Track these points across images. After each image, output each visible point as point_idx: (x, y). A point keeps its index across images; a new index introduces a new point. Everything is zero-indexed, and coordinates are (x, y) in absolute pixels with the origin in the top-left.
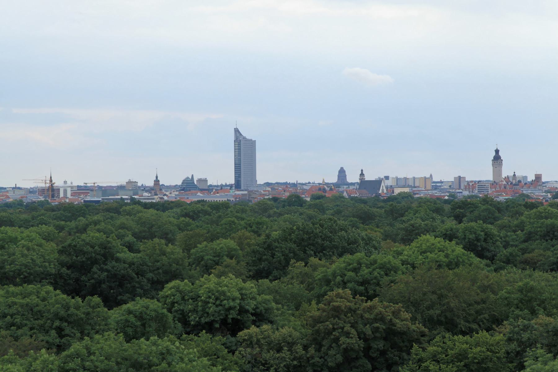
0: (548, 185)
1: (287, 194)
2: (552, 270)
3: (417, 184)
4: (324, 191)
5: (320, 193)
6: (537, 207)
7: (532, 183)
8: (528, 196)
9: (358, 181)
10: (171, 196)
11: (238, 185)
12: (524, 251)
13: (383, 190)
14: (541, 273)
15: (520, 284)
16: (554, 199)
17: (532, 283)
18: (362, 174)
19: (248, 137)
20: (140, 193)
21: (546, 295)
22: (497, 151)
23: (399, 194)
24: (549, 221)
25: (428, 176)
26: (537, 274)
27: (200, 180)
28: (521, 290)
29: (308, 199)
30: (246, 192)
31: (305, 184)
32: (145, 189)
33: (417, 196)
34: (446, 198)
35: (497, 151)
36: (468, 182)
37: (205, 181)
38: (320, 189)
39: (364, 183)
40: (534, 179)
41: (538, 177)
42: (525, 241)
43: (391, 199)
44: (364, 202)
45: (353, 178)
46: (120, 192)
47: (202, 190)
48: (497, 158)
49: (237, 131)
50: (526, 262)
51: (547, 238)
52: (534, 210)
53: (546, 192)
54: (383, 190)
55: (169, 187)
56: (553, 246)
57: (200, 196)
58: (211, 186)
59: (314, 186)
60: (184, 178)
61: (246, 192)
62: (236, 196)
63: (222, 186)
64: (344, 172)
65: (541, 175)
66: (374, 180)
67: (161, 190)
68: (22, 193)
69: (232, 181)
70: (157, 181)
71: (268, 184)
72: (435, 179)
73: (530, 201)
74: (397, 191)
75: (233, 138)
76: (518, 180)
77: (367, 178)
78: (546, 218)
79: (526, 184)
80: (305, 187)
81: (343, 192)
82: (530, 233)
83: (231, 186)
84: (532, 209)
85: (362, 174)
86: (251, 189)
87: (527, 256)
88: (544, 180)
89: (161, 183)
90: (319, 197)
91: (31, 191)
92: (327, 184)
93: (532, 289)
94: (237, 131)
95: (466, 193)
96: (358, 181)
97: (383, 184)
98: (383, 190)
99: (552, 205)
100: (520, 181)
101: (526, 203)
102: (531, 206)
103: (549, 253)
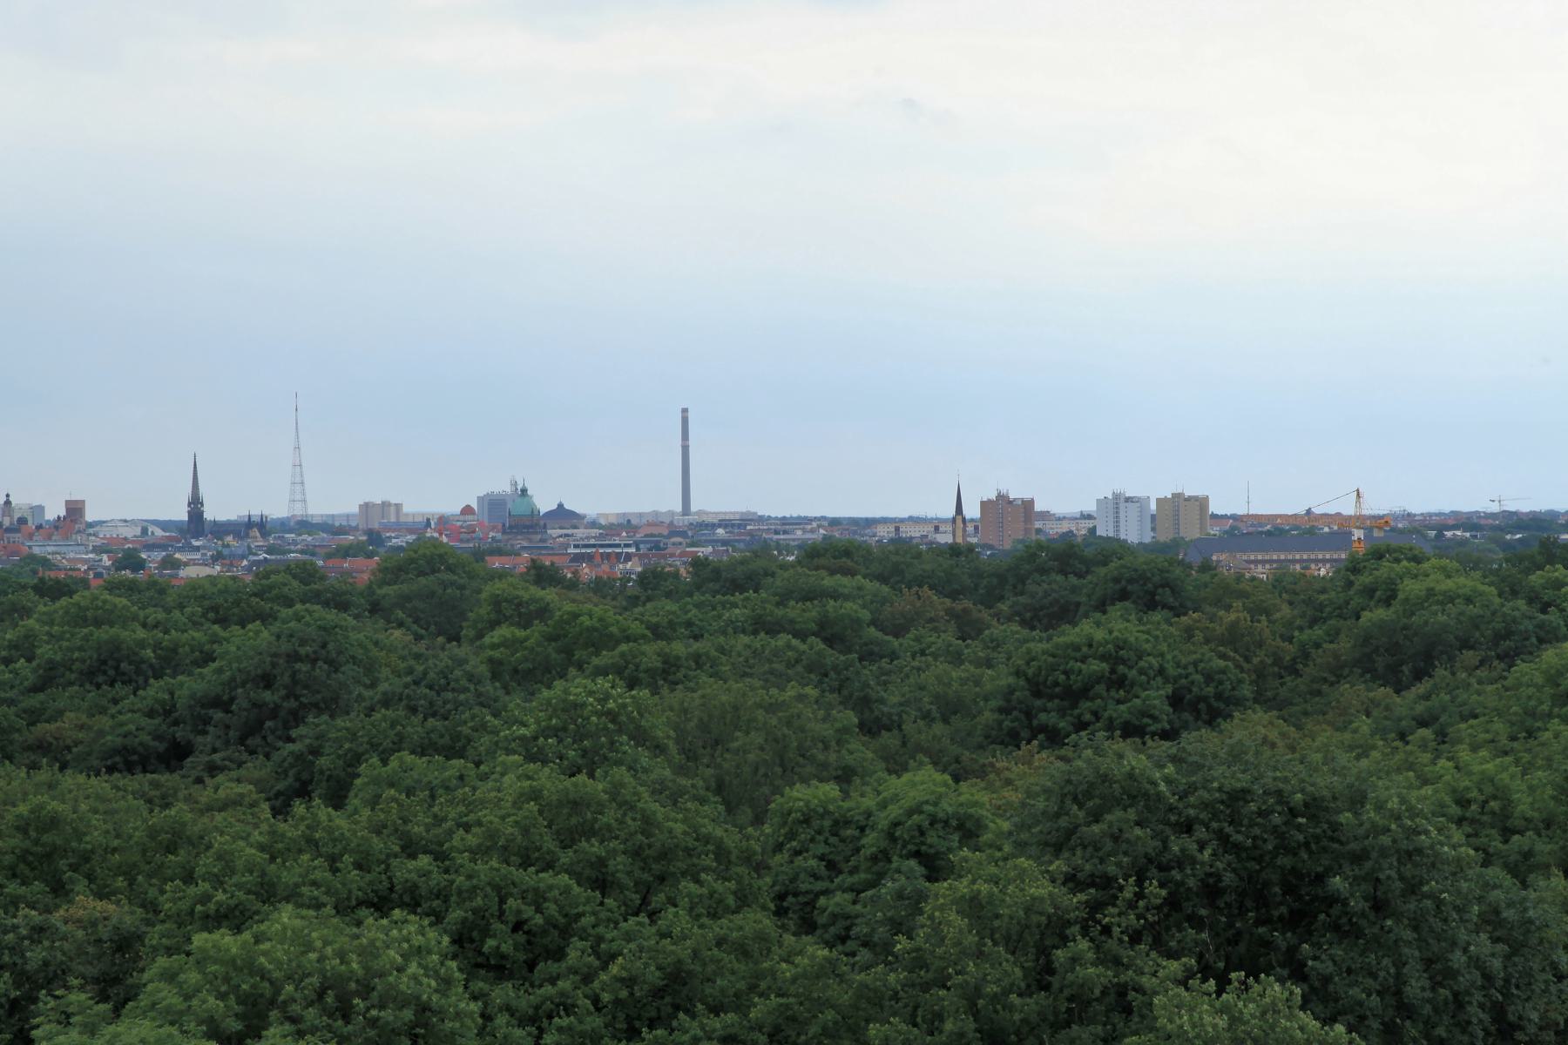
0: (104, 532)
2: (111, 770)
6: (71, 593)
7: (58, 524)
8: (45, 562)
12: (34, 717)
14: (81, 778)
15: (23, 809)
16: (118, 569)
17: (54, 805)
21: (95, 837)
24: (104, 633)
26: (71, 780)
28: (22, 828)
40: (63, 513)
41: (75, 510)
42: (36, 689)
50: (42, 747)
51: (101, 679)
52: (64, 601)
53: (96, 550)
56: (115, 701)
65: (83, 502)
73: (53, 575)
76: (17, 516)
78: (98, 623)
79: (39, 527)
82: (52, 666)
84: (54, 599)
87: (43, 728)
88: (90, 516)
93: (54, 822)
99: (112, 587)
100: (22, 521)
101: (42, 580)
102: (54, 590)
103: (105, 722)
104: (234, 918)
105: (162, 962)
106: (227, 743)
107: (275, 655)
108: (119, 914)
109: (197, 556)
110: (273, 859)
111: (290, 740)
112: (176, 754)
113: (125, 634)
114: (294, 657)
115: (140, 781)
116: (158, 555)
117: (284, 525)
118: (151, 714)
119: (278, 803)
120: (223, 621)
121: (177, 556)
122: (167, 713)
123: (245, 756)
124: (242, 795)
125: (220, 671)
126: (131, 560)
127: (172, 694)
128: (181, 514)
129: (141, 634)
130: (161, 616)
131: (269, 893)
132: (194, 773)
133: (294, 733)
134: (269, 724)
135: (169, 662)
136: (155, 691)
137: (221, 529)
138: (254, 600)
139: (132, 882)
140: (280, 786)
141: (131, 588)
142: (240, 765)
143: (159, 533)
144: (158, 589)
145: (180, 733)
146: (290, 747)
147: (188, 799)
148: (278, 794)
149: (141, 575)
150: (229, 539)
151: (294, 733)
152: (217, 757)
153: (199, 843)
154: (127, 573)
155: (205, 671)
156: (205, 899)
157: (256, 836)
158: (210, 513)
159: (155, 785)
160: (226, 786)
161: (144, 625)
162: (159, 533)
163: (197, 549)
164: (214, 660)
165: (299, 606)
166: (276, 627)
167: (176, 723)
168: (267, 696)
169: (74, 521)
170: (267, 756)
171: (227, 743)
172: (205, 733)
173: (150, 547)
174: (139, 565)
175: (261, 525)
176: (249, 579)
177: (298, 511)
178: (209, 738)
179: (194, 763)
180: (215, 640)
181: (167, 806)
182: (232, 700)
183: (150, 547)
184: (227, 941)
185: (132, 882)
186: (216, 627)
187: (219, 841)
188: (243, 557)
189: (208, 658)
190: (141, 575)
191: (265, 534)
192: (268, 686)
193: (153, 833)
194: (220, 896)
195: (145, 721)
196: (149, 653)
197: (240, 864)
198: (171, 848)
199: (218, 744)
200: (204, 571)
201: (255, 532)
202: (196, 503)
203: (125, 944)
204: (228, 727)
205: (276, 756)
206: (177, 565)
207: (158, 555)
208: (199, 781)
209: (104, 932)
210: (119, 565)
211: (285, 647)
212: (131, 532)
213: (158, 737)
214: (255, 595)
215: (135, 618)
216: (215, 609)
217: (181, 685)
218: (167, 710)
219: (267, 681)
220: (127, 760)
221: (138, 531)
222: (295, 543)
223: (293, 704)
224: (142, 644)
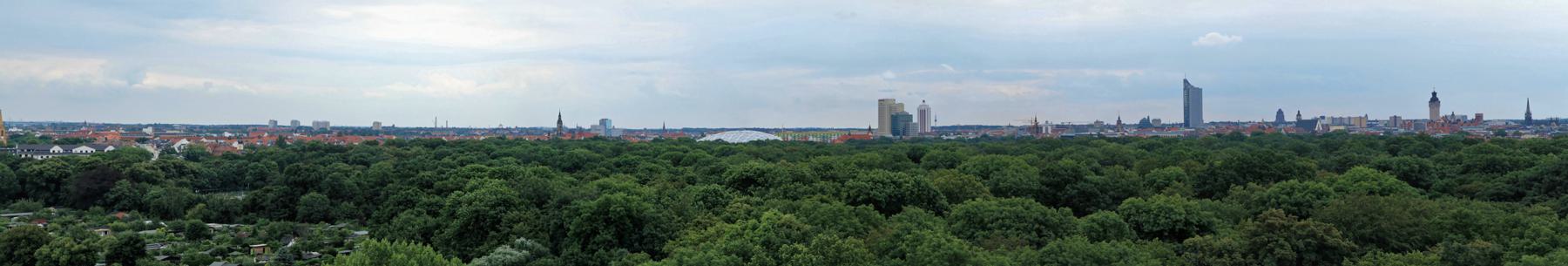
1: (1230, 131)
2: (1491, 200)
3: (1352, 123)
4: (1264, 128)
5: (1260, 130)
6: (1477, 143)
7: (1472, 121)
8: (1467, 133)
10: (1132, 132)
11: (1186, 124)
12: (1462, 182)
13: (1319, 127)
14: (1480, 202)
15: (1455, 211)
17: (1466, 210)
18: (1299, 115)
19: (1196, 86)
21: (1483, 221)
22: (1434, 94)
23: (1335, 131)
24: (1489, 156)
25: (1363, 116)
26: (1475, 203)
27: (1154, 120)
28: (1455, 217)
29: (1249, 135)
31: (1247, 123)
32: (1109, 127)
34: (1382, 134)
35: (1434, 94)
36: (1404, 121)
37: (1159, 120)
38: (1259, 127)
39: (1300, 122)
41: (1479, 117)
42: (1463, 173)
44: (1300, 138)
45: (1290, 117)
46: (1090, 129)
47: (1156, 128)
48: (1434, 100)
50: (1465, 192)
52: (1475, 146)
53: (1487, 129)
55: (1130, 126)
56: (1494, 178)
58: (1163, 125)
59: (1253, 125)
62: (1185, 133)
64: (1282, 112)
66: (1310, 119)
68: (1014, 129)
69: (1182, 121)
70: (1119, 121)
71: (1213, 123)
74: (1333, 129)
76: (1457, 118)
77: (1304, 117)
78: (1486, 153)
79: (1465, 122)
80: (1246, 125)
81: (1281, 130)
82: (1469, 166)
83: (1181, 125)
84: (1470, 145)
85: (1299, 115)
87: (1464, 186)
88: (1485, 118)
90: (1258, 134)
91: (1021, 129)
92: (1266, 123)
93: (1467, 215)
95: (1402, 130)
98: (1319, 128)
100: (1459, 120)
103: (1490, 184)
106: (1540, 193)
108: (1493, 246)
110: (1557, 232)
112: (1518, 196)
113: (1497, 157)
115: (1504, 204)
116: (1513, 131)
118: (1508, 183)
120: (1539, 153)
125: (1537, 169)
127: (1517, 176)
128: (1522, 117)
130: (1512, 151)
131: (1555, 244)
132: (1526, 203)
134: (1558, 188)
136: (1510, 175)
137: (1539, 123)
139: (1498, 236)
140: (1562, 209)
141: (1501, 142)
142: (1545, 201)
143: (1513, 124)
144: (1512, 143)
145: (1520, 189)
147: (1523, 211)
148: (1562, 211)
152: (1536, 198)
153: (1526, 226)
154: (1500, 137)
155: (1531, 169)
156: (1528, 244)
157: (1551, 225)
160: (1538, 207)
166: (1561, 155)
167: (1518, 186)
168: (1557, 178)
169: (1479, 121)
170: (1558, 198)
171: (1540, 193)
172: (1531, 189)
174: (1506, 134)
175: (1557, 121)
176: (1550, 139)
179: (1528, 199)
180: (1535, 159)
182: (1542, 179)
184: (1537, 259)
185: (1498, 236)
186: (1536, 155)
187: (1533, 226)
189: (1532, 165)
193: (1507, 221)
194: (1535, 244)
195: (1505, 185)
196: (1507, 163)
197: (1542, 233)
198: (1514, 227)
200: (1533, 136)
202: (1528, 114)
203: (1496, 256)
205: (1561, 198)
206: (1521, 134)
207: (1513, 131)
208: (1528, 205)
210: (1496, 135)
212: (1501, 124)
213: (1512, 191)
215: (1502, 152)
216: (1535, 149)
218: (1515, 182)
219: (1558, 173)
220: (1498, 197)
224: (1504, 160)
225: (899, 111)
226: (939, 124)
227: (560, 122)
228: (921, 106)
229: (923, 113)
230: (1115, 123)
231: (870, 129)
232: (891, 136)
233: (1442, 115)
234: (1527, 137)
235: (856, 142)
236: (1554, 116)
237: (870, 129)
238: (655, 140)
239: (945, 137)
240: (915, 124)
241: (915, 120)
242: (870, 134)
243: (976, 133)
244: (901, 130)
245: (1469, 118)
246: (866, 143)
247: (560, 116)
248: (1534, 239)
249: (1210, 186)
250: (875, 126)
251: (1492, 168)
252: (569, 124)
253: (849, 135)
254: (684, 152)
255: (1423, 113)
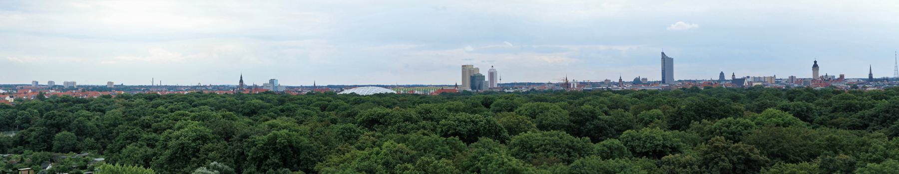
1: (691, 86)
2: (849, 129)
3: (766, 81)
4: (712, 84)
5: (709, 85)
6: (840, 93)
7: (838, 79)
8: (835, 87)
9: (731, 79)
10: (628, 87)
11: (663, 81)
12: (832, 118)
13: (746, 83)
14: (842, 130)
15: (828, 136)
16: (852, 88)
17: (834, 136)
18: (733, 75)
19: (669, 57)
20: (612, 85)
21: (845, 142)
22: (815, 62)
23: (756, 86)
24: (848, 102)
25: (773, 76)
26: (840, 131)
27: (643, 79)
28: (828, 140)
29: (703, 89)
30: (668, 85)
33: (766, 87)
34: (784, 88)
35: (815, 62)
36: (797, 79)
37: (646, 79)
38: (709, 83)
39: (734, 80)
40: (839, 77)
41: (842, 76)
42: (832, 112)
43: (750, 88)
44: (735, 90)
45: (728, 77)
46: (602, 85)
47: (644, 84)
48: (815, 66)
49: (663, 53)
50: (833, 124)
51: (847, 111)
52: (839, 95)
53: (847, 84)
54: (746, 83)
56: (851, 115)
57: (643, 87)
60: (635, 78)
61: (668, 85)
62: (662, 87)
63: (655, 82)
65: (844, 75)
67: (623, 84)
68: (552, 85)
69: (661, 80)
70: (620, 80)
71: (680, 81)
72: (777, 78)
73: (837, 89)
74: (754, 84)
75: (661, 57)
76: (829, 78)
77: (737, 77)
78: (846, 99)
80: (701, 82)
83: (660, 82)
84: (836, 94)
85: (733, 75)
86: (670, 83)
88: (845, 78)
89: (623, 81)
90: (709, 88)
91: (557, 85)
92: (713, 81)
93: (835, 139)
94: (663, 53)
95: (796, 85)
96: (731, 79)
97: (746, 81)
98: (746, 84)
99: (850, 92)
100: (830, 79)
101: (834, 91)
102: (836, 92)
103: (848, 119)
104: (878, 161)
105: (859, 169)
107: (890, 106)
108: (850, 158)
109: (871, 86)
110: (887, 149)
111: (893, 124)
112: (865, 126)
113: (853, 102)
114: (895, 107)
115: (857, 131)
116: (862, 86)
117: (893, 79)
118: (859, 118)
119: (890, 137)
120: (877, 99)
121: (866, 86)
122: (863, 118)
123: (882, 127)
124: (881, 135)
125: (876, 109)
126: (855, 87)
127: (864, 114)
129: (856, 101)
130: (861, 98)
131: (886, 156)
132: (869, 130)
133: (894, 123)
135: (863, 107)
136: (860, 113)
137: (877, 80)
138: (884, 95)
139: (853, 152)
140: (890, 134)
141: (855, 92)
143: (862, 81)
144: (861, 93)
145: (866, 122)
146: (893, 126)
147: (868, 135)
148: (890, 136)
149: (857, 90)
150: (879, 82)
151: (894, 123)
152: (875, 127)
153: (869, 145)
154: (854, 89)
155: (872, 109)
156: (870, 156)
157: (884, 144)
158: (874, 77)
159: (860, 132)
160: (876, 133)
161: (857, 100)
162: (862, 81)
163: (871, 84)
164: (874, 107)
165: (895, 96)
166: (889, 101)
168: (888, 115)
170: (888, 128)
171: (878, 124)
172: (872, 122)
173: (860, 84)
174: (857, 88)
175: (887, 79)
177: (896, 76)
178: (873, 123)
180: (874, 103)
181: (862, 137)
182: (879, 115)
183: (860, 84)
184: (876, 166)
185: (853, 152)
186: (875, 101)
187: (874, 145)
188: (883, 86)
189: (873, 107)
190: (857, 90)
191: (888, 81)
192: (888, 113)
193: (858, 142)
194: (874, 156)
195: (857, 120)
196: (858, 106)
197: (879, 150)
198: (862, 145)
199: (875, 124)
200: (873, 89)
201: (885, 81)
202: (871, 75)
203: (852, 165)
204: (877, 121)
205: (890, 127)
206: (866, 87)
207: (862, 86)
208: (871, 132)
209: (847, 162)
210: (852, 88)
211: (892, 105)
212: (854, 81)
214: (885, 94)
215: (855, 98)
216: (875, 97)
217: (866, 112)
218: (863, 117)
219: (888, 112)
220: (853, 127)
221: (857, 80)
222: (895, 83)
223: (894, 117)
224: (857, 104)
225: (476, 73)
226: (503, 82)
227: (241, 81)
228: (490, 70)
229: (492, 75)
230: (617, 81)
231: (456, 86)
232: (470, 90)
233: (820, 75)
234: (870, 89)
235: (447, 94)
236: (885, 76)
237: (456, 86)
238: (309, 94)
239: (506, 91)
240: (487, 82)
241: (487, 79)
242: (456, 89)
243: (527, 88)
244: (477, 86)
245: (836, 78)
246: (453, 95)
247: (241, 77)
248: (874, 153)
249: (678, 122)
250: (460, 83)
251: (850, 109)
252: (248, 82)
253: (442, 89)
254: (329, 102)
255: (808, 74)
